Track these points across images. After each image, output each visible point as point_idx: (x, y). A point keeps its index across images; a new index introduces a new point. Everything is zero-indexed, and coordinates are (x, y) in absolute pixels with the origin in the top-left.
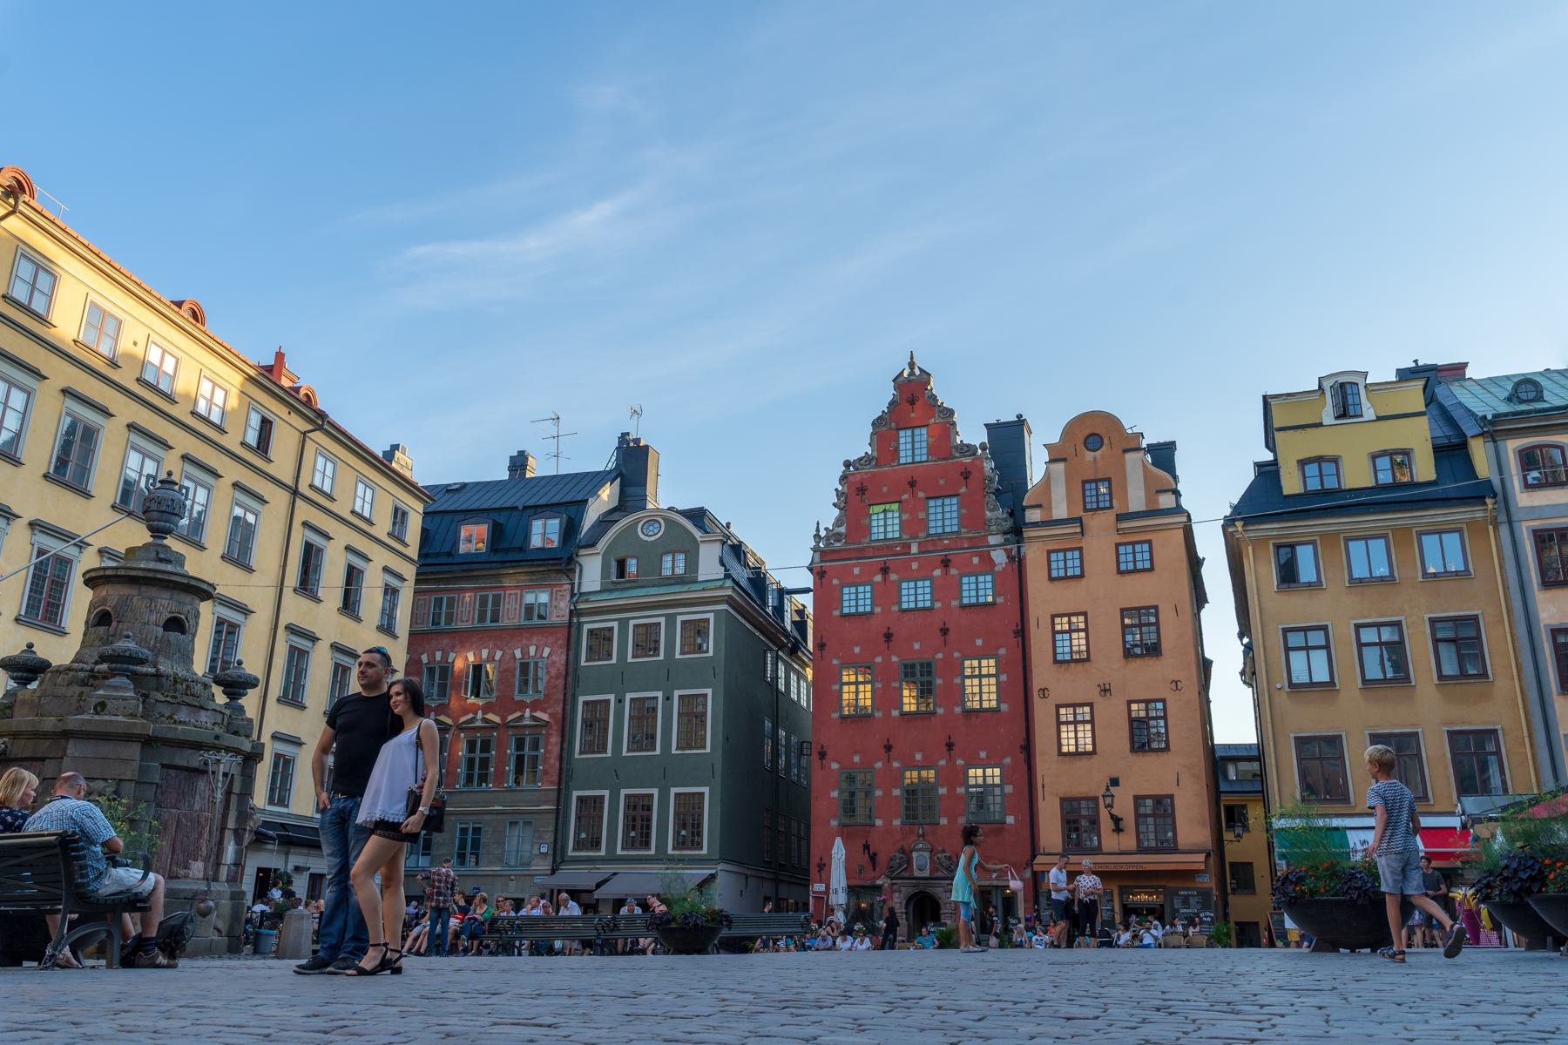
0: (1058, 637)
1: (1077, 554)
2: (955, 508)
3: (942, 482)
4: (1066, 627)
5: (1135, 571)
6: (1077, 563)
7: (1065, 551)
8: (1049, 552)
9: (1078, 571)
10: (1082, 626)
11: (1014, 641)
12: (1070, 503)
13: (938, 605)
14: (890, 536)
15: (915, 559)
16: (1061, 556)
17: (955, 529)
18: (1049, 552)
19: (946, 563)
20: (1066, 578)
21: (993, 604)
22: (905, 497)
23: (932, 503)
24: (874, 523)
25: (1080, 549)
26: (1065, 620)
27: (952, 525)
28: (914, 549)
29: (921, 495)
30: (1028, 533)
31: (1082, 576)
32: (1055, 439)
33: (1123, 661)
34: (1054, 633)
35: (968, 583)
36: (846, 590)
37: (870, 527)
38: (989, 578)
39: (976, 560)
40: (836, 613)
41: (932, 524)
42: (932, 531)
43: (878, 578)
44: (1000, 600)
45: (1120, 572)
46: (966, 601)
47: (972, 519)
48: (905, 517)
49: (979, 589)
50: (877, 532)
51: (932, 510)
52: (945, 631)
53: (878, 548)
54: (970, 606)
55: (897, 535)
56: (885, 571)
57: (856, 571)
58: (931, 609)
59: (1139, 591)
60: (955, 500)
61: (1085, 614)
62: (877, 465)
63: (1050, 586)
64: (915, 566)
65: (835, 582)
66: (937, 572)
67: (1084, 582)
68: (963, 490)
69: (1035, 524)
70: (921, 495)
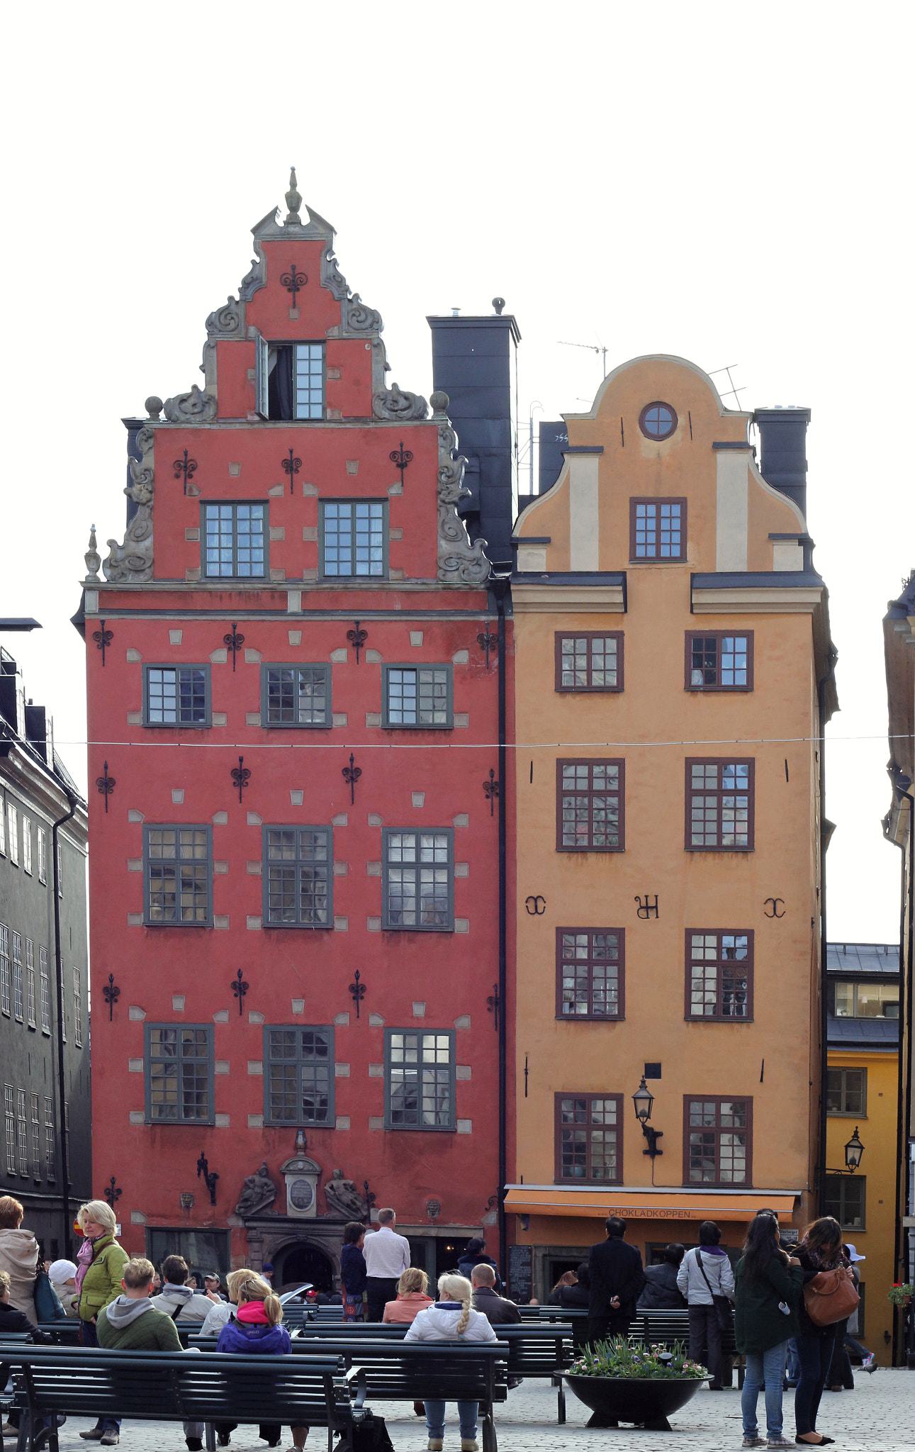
1: (612, 644)
2: (377, 526)
3: (352, 468)
4: (583, 785)
6: (612, 663)
7: (590, 636)
8: (560, 636)
11: (484, 804)
12: (604, 541)
14: (243, 571)
15: (296, 625)
17: (377, 570)
18: (560, 636)
19: (357, 639)
20: (589, 690)
22: (277, 491)
23: (330, 510)
24: (213, 541)
25: (619, 636)
26: (583, 771)
27: (371, 564)
28: (294, 603)
30: (520, 594)
31: (618, 689)
33: (683, 856)
34: (561, 794)
35: (401, 687)
37: (203, 548)
39: (417, 638)
41: (330, 554)
42: (331, 570)
43: (221, 656)
44: (461, 722)
46: (394, 718)
47: (409, 546)
48: (277, 534)
50: (218, 562)
51: (330, 526)
52: (352, 774)
53: (220, 595)
54: (405, 729)
55: (259, 571)
56: (234, 642)
57: (176, 637)
58: (324, 729)
59: (719, 726)
60: (377, 510)
61: (620, 763)
64: (295, 638)
65: (132, 656)
66: (340, 656)
67: (621, 700)
69: (534, 577)
70: (310, 491)
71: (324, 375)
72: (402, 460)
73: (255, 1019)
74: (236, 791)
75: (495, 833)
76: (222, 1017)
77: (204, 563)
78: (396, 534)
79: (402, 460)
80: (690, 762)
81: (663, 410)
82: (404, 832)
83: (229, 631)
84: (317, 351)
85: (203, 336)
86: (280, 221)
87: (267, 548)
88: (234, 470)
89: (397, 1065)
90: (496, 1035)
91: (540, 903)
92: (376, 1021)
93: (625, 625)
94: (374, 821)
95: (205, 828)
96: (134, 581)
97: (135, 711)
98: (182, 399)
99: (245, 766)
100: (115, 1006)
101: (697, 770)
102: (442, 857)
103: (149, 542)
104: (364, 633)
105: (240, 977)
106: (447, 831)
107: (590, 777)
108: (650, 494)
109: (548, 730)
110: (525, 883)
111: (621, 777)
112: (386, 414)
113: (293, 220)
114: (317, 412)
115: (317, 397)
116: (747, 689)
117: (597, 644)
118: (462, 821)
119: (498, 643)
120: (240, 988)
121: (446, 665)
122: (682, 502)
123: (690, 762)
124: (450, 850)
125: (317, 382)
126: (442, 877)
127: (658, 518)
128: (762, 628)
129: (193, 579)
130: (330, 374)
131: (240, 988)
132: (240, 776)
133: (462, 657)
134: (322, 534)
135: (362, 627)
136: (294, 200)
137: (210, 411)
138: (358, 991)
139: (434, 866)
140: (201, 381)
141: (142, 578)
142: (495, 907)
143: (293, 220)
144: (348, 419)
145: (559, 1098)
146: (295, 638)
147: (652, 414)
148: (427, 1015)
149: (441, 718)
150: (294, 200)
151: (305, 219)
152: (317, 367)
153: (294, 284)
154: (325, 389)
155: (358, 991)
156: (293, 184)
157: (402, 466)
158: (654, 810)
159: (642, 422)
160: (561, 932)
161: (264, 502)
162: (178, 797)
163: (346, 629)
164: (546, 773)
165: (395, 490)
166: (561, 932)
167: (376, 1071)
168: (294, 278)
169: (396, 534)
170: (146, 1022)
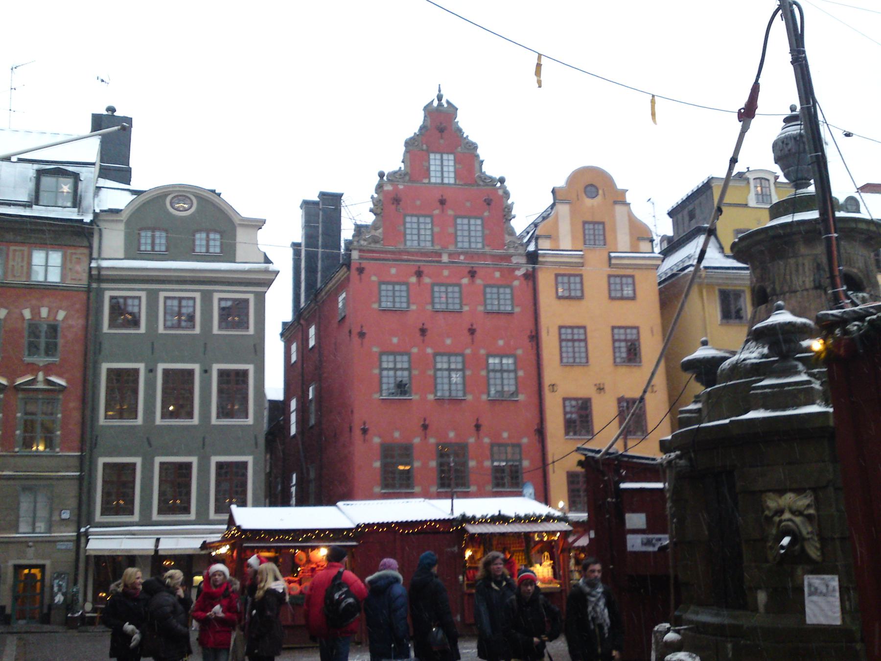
0: (564, 344)
2: (479, 228)
3: (468, 204)
4: (569, 337)
5: (622, 298)
6: (578, 286)
7: (570, 275)
8: (557, 276)
9: (579, 294)
10: (582, 337)
13: (466, 308)
16: (566, 279)
19: (472, 274)
20: (569, 298)
21: (510, 314)
22: (437, 212)
23: (459, 221)
25: (581, 276)
26: (569, 331)
28: (445, 258)
29: (450, 212)
31: (581, 298)
32: (560, 182)
34: (561, 341)
36: (383, 287)
37: (405, 234)
38: (508, 291)
39: (497, 274)
40: (375, 306)
41: (459, 239)
43: (413, 280)
44: (517, 310)
45: (612, 298)
46: (489, 307)
48: (437, 229)
49: (501, 300)
51: (459, 227)
56: (419, 274)
57: (393, 271)
61: (584, 328)
62: (411, 180)
63: (558, 302)
65: (374, 278)
67: (584, 302)
68: (486, 214)
71: (455, 166)
72: (488, 202)
73: (432, 440)
74: (422, 338)
75: (533, 357)
76: (417, 440)
77: (405, 241)
78: (487, 232)
79: (488, 202)
80: (613, 328)
81: (593, 189)
82: (494, 356)
83: (417, 269)
84: (451, 157)
85: (404, 149)
86: (436, 103)
87: (433, 235)
88: (418, 203)
89: (496, 461)
90: (538, 446)
91: (555, 388)
92: (487, 440)
93: (584, 271)
94: (483, 352)
95: (408, 354)
96: (373, 246)
97: (374, 302)
98: (395, 173)
99: (425, 327)
100: (367, 437)
101: (616, 331)
102: (512, 367)
103: (380, 230)
104: (475, 272)
105: (425, 420)
106: (515, 357)
107: (573, 334)
108: (590, 219)
109: (554, 314)
110: (549, 376)
111: (585, 333)
112: (481, 183)
113: (440, 105)
114: (452, 181)
115: (452, 175)
116: (633, 298)
117: (572, 279)
118: (519, 352)
119: (531, 277)
120: (425, 427)
121: (510, 286)
122: (603, 223)
123: (613, 328)
124: (515, 363)
125: (452, 169)
126: (512, 375)
127: (594, 230)
128: (638, 274)
129: (402, 247)
130: (457, 166)
131: (425, 427)
132: (423, 331)
133: (516, 283)
134: (456, 230)
135: (475, 269)
136: (440, 98)
137: (407, 178)
138: (478, 427)
139: (508, 371)
140: (402, 166)
141: (378, 246)
142: (535, 388)
143: (440, 105)
144: (466, 184)
145: (568, 473)
146: (446, 273)
147: (589, 188)
148: (509, 437)
149: (509, 308)
150: (440, 98)
151: (446, 105)
152: (452, 163)
153: (441, 130)
154: (456, 172)
155: (478, 427)
156: (440, 91)
157: (489, 204)
158: (600, 347)
159: (585, 192)
160: (565, 399)
161: (431, 216)
162: (395, 340)
163: (468, 269)
164: (554, 332)
165: (486, 214)
166: (565, 399)
167: (487, 463)
168: (440, 129)
169: (487, 232)
170: (382, 444)
